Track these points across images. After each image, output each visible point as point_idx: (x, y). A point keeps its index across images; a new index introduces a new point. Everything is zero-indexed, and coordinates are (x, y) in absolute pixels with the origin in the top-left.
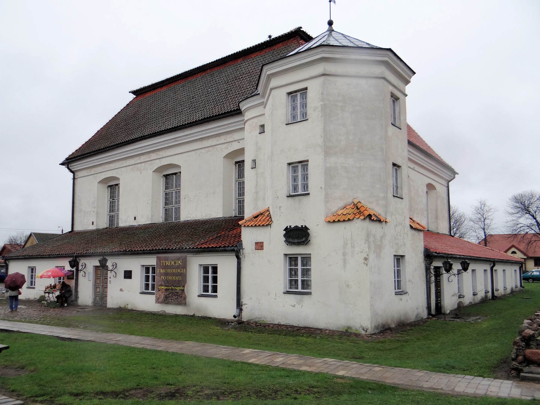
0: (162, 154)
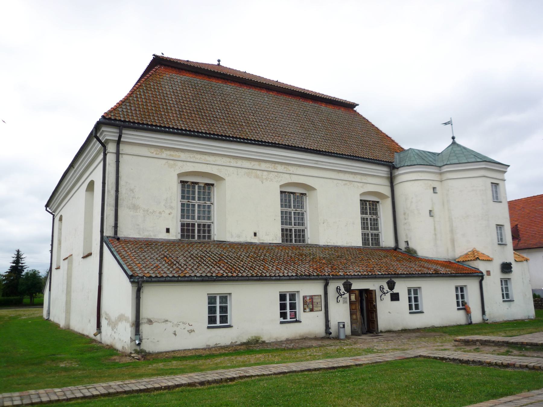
0: (292, 169)
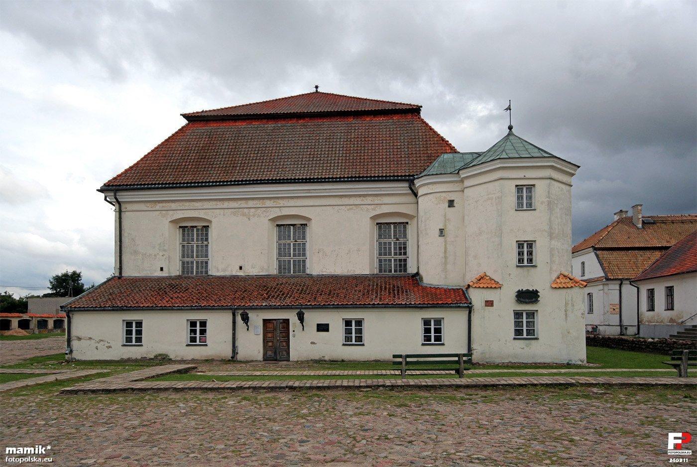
0: (282, 203)
